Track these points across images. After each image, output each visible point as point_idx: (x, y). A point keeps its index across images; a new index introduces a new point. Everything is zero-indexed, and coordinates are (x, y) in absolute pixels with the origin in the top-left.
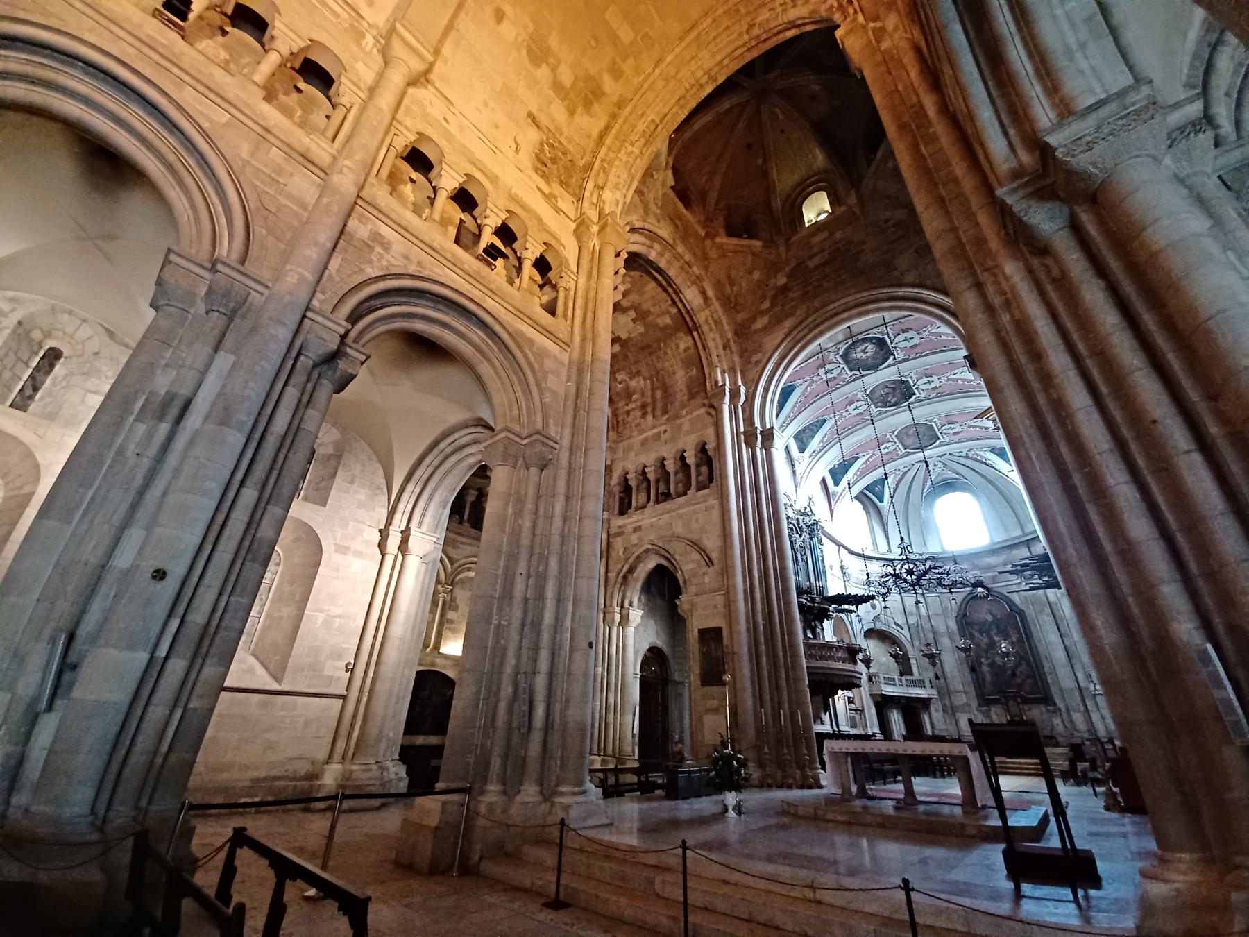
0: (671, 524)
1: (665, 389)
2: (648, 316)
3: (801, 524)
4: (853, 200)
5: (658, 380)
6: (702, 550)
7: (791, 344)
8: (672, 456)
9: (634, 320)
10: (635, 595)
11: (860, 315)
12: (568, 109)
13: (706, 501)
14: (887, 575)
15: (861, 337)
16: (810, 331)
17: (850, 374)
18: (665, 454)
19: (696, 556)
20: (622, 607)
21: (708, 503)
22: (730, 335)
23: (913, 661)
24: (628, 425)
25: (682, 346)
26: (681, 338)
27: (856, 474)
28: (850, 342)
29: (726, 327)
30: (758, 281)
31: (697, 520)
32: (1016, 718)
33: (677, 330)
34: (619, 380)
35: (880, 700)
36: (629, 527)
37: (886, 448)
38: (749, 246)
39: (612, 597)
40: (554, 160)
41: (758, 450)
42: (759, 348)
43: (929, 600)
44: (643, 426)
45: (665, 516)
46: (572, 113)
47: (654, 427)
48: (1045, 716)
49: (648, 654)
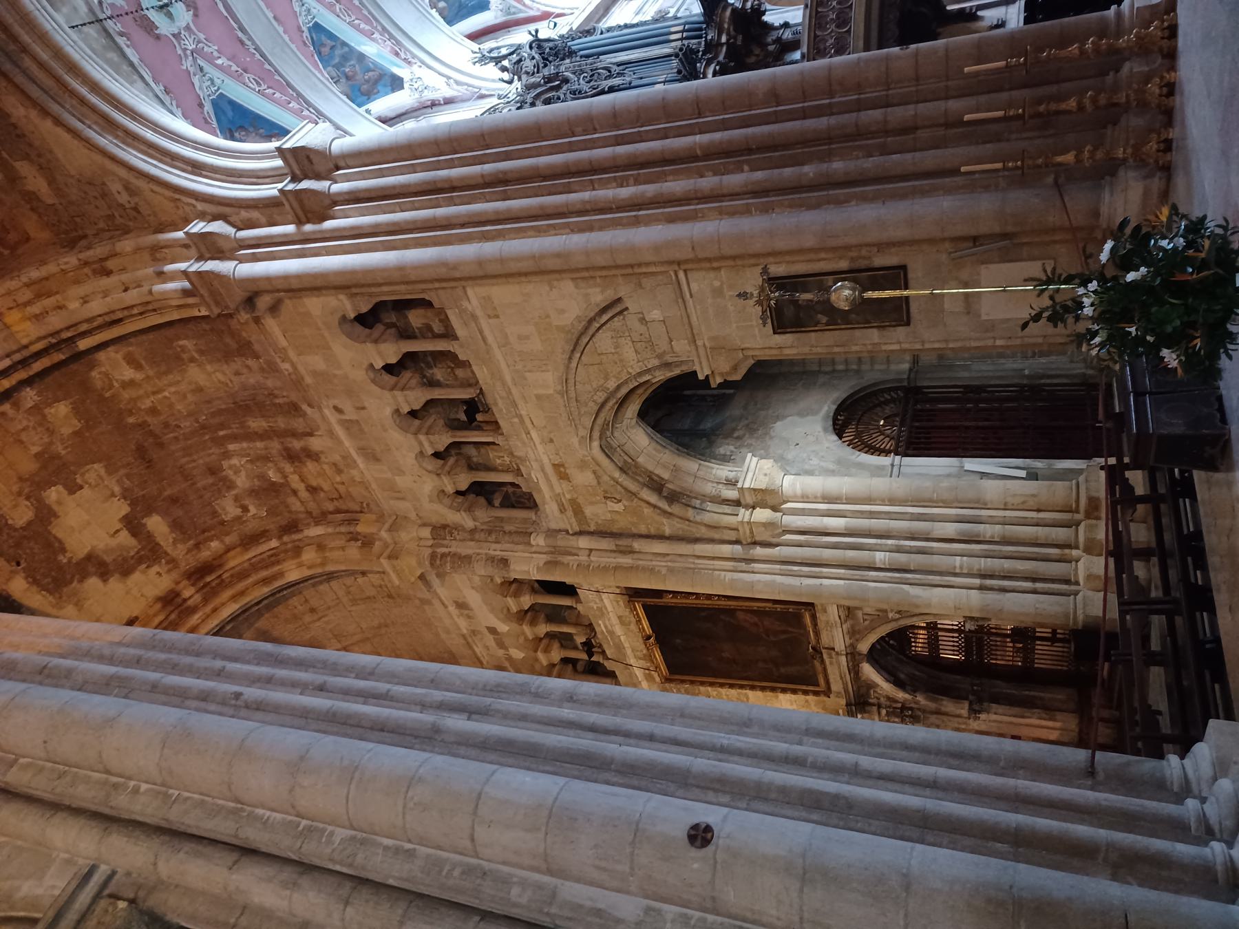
3: (537, 79)
5: (222, 426)
8: (387, 394)
9: (73, 488)
13: (474, 317)
16: (24, 49)
18: (388, 411)
20: (737, 503)
24: (342, 489)
25: (128, 373)
33: (85, 386)
34: (238, 511)
36: (558, 490)
44: (336, 458)
45: (523, 413)
47: (331, 433)
49: (849, 434)
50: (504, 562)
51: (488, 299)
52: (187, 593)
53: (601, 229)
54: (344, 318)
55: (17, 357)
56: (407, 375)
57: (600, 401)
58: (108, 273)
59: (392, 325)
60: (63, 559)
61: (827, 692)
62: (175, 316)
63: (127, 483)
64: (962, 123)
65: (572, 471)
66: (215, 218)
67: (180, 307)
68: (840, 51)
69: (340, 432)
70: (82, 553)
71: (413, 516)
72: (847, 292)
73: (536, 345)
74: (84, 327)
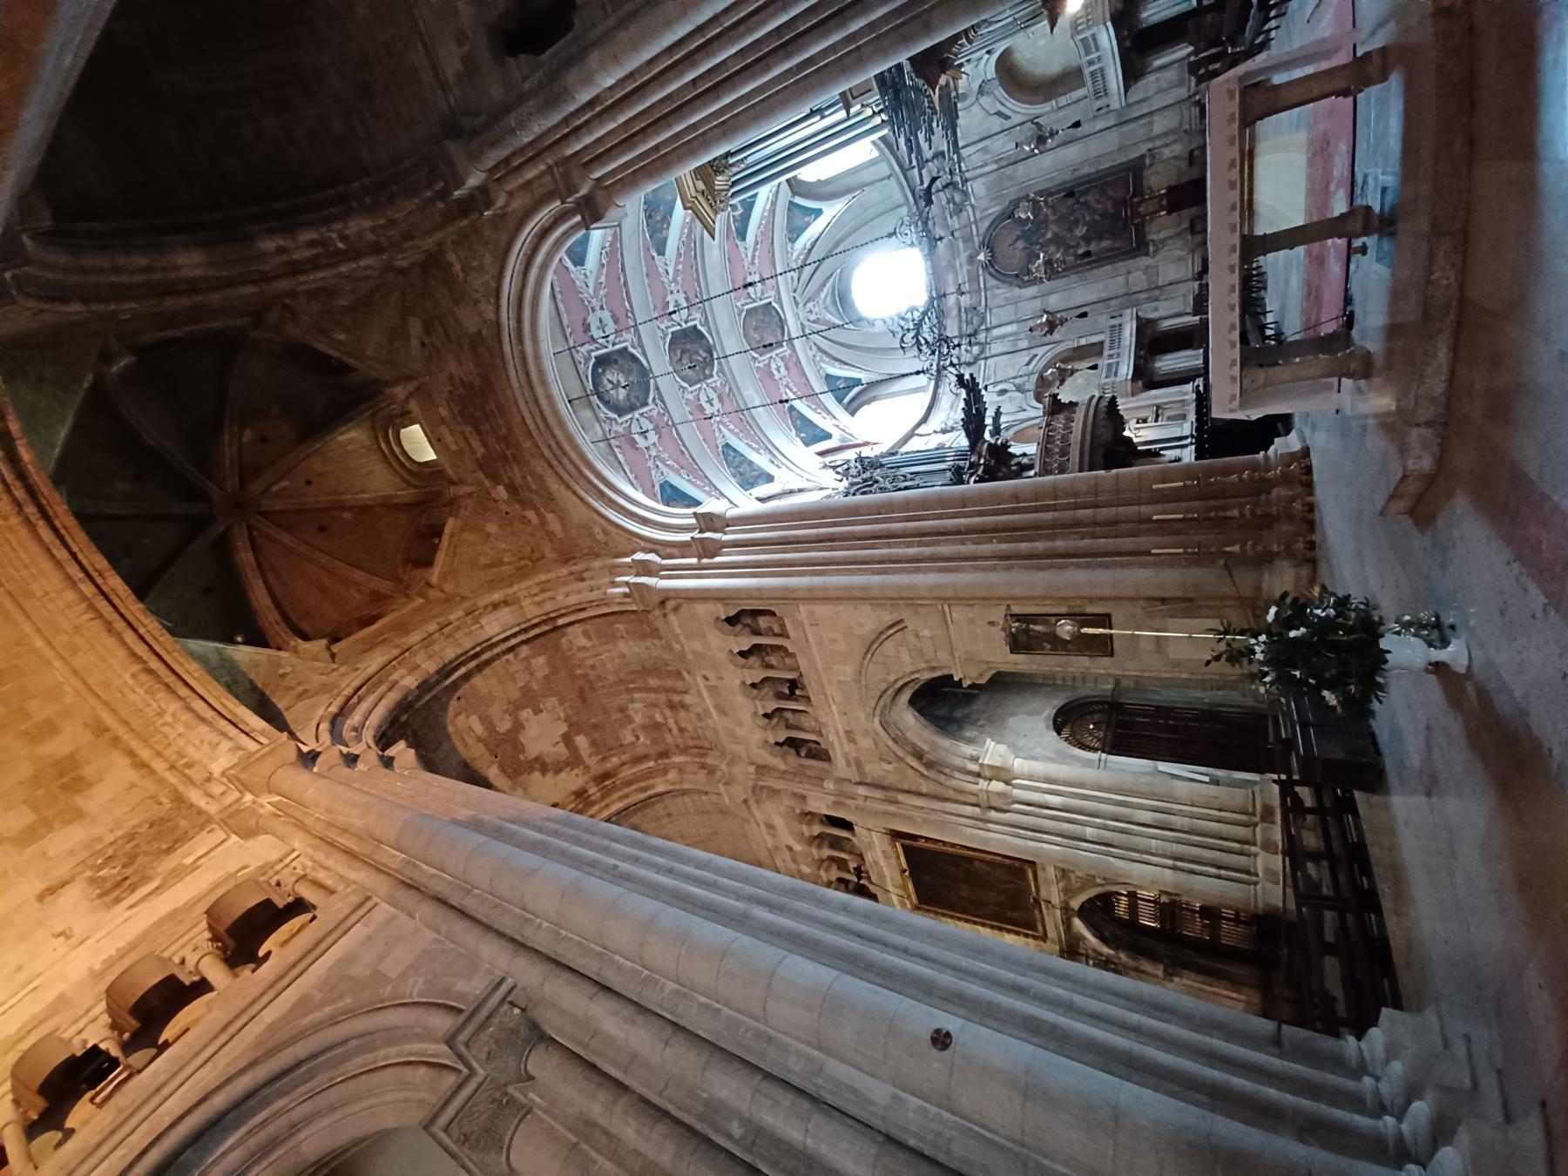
0: (840, 682)
1: (647, 671)
2: (531, 690)
3: (858, 480)
4: (399, 391)
6: (880, 637)
7: (582, 482)
9: (537, 711)
10: (959, 751)
11: (544, 383)
12: (67, 823)
13: (802, 625)
14: (918, 341)
15: (590, 386)
16: (565, 453)
17: (652, 406)
18: (738, 682)
19: (889, 647)
20: (978, 775)
21: (805, 622)
22: (565, 571)
23: (1083, 342)
24: (700, 732)
25: (583, 641)
26: (571, 642)
27: (815, 410)
28: (595, 399)
29: (553, 575)
30: (501, 527)
31: (833, 641)
32: (1164, 202)
33: (557, 647)
34: (633, 739)
35: (1140, 383)
36: (847, 750)
37: (778, 369)
38: (452, 536)
39: (961, 792)
40: (131, 859)
41: (725, 538)
42: (587, 529)
43: (995, 322)
44: (700, 710)
45: (828, 692)
46: (78, 815)
47: (699, 694)
48: (1160, 168)
49: (1066, 732)
50: (803, 798)
51: (811, 614)
52: (591, 791)
53: (893, 573)
54: (718, 618)
55: (523, 626)
56: (753, 660)
57: (882, 688)
58: (583, 580)
59: (747, 625)
60: (522, 757)
61: (1044, 938)
62: (616, 609)
63: (569, 711)
64: (1150, 520)
65: (859, 738)
66: (651, 551)
67: (620, 604)
68: (1062, 471)
69: (705, 693)
70: (533, 756)
71: (744, 756)
72: (1069, 628)
73: (841, 646)
74: (563, 611)
